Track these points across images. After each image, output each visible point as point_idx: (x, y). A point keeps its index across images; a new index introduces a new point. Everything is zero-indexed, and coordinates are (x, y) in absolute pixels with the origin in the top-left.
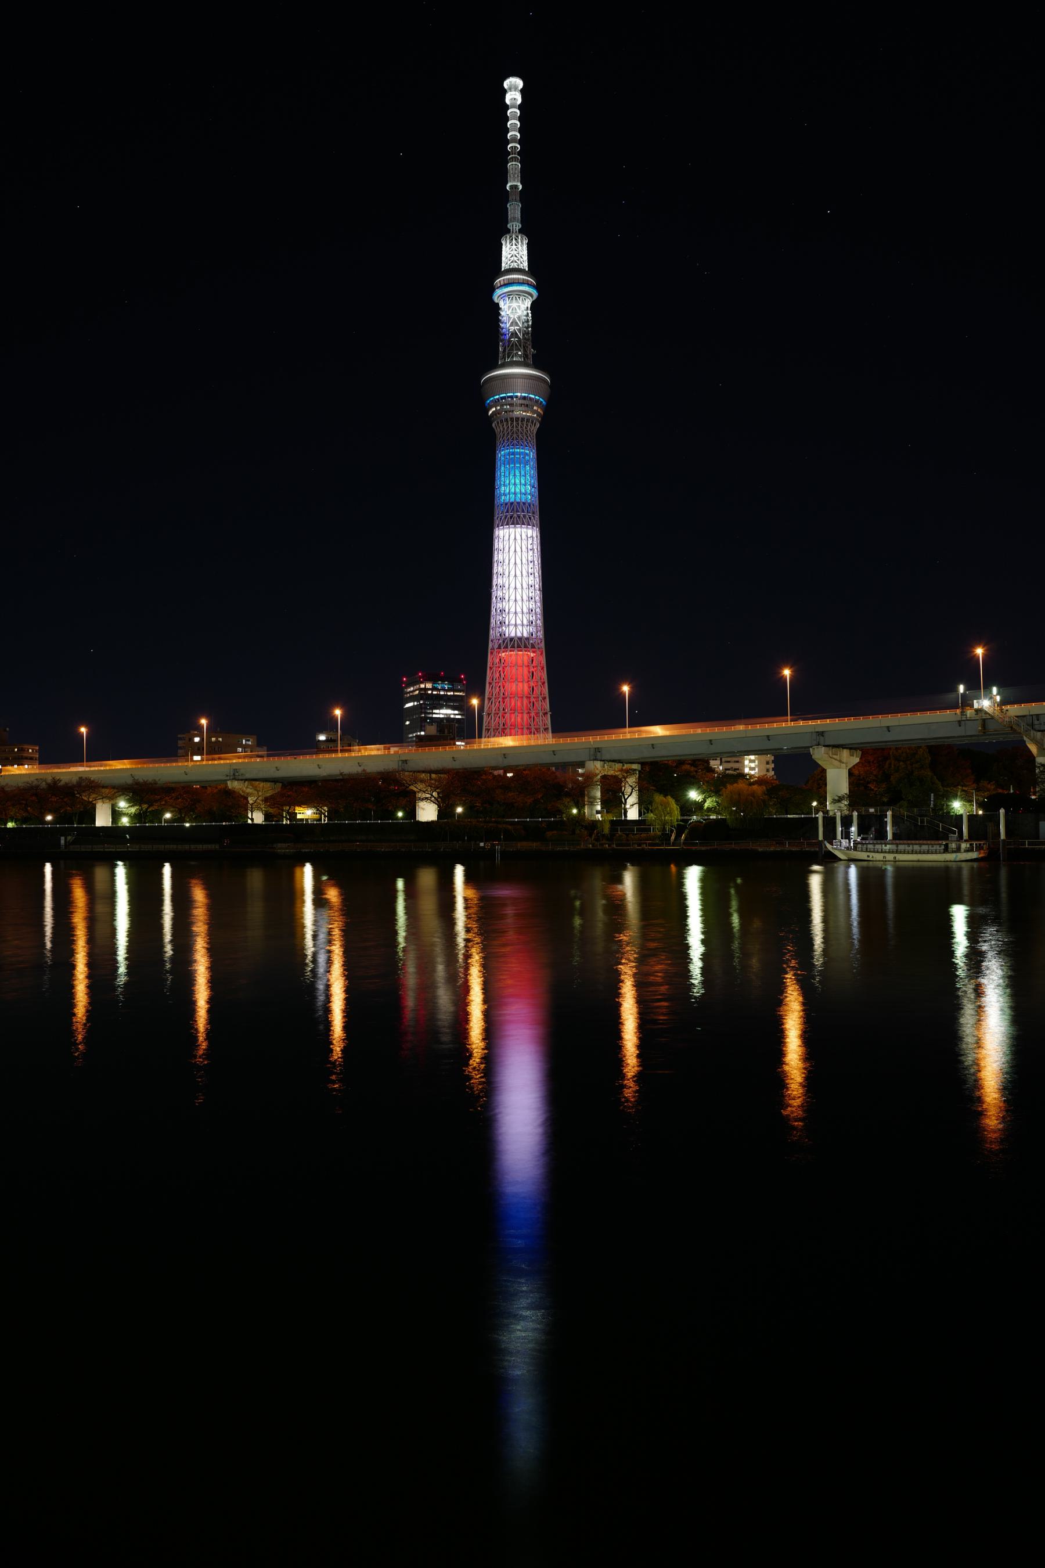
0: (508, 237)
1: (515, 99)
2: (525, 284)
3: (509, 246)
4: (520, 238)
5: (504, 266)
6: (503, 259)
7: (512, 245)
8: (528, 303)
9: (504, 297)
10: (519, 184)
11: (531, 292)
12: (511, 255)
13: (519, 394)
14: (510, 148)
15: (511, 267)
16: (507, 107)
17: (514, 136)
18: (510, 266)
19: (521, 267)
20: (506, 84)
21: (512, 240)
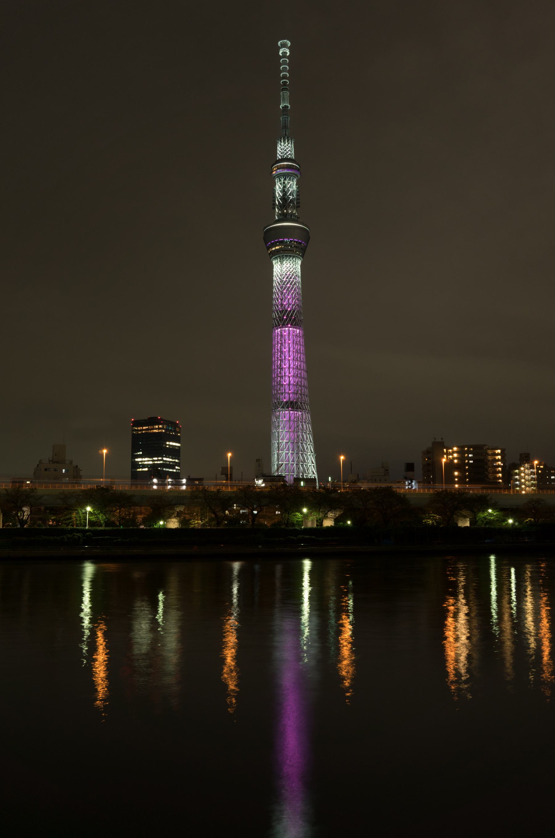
1: (285, 52)
2: (293, 169)
3: (282, 144)
4: (290, 138)
6: (278, 152)
7: (285, 143)
8: (295, 180)
9: (281, 176)
10: (288, 105)
11: (295, 173)
13: (286, 240)
14: (282, 82)
16: (281, 57)
17: (284, 75)
18: (284, 156)
20: (279, 43)
21: (285, 140)
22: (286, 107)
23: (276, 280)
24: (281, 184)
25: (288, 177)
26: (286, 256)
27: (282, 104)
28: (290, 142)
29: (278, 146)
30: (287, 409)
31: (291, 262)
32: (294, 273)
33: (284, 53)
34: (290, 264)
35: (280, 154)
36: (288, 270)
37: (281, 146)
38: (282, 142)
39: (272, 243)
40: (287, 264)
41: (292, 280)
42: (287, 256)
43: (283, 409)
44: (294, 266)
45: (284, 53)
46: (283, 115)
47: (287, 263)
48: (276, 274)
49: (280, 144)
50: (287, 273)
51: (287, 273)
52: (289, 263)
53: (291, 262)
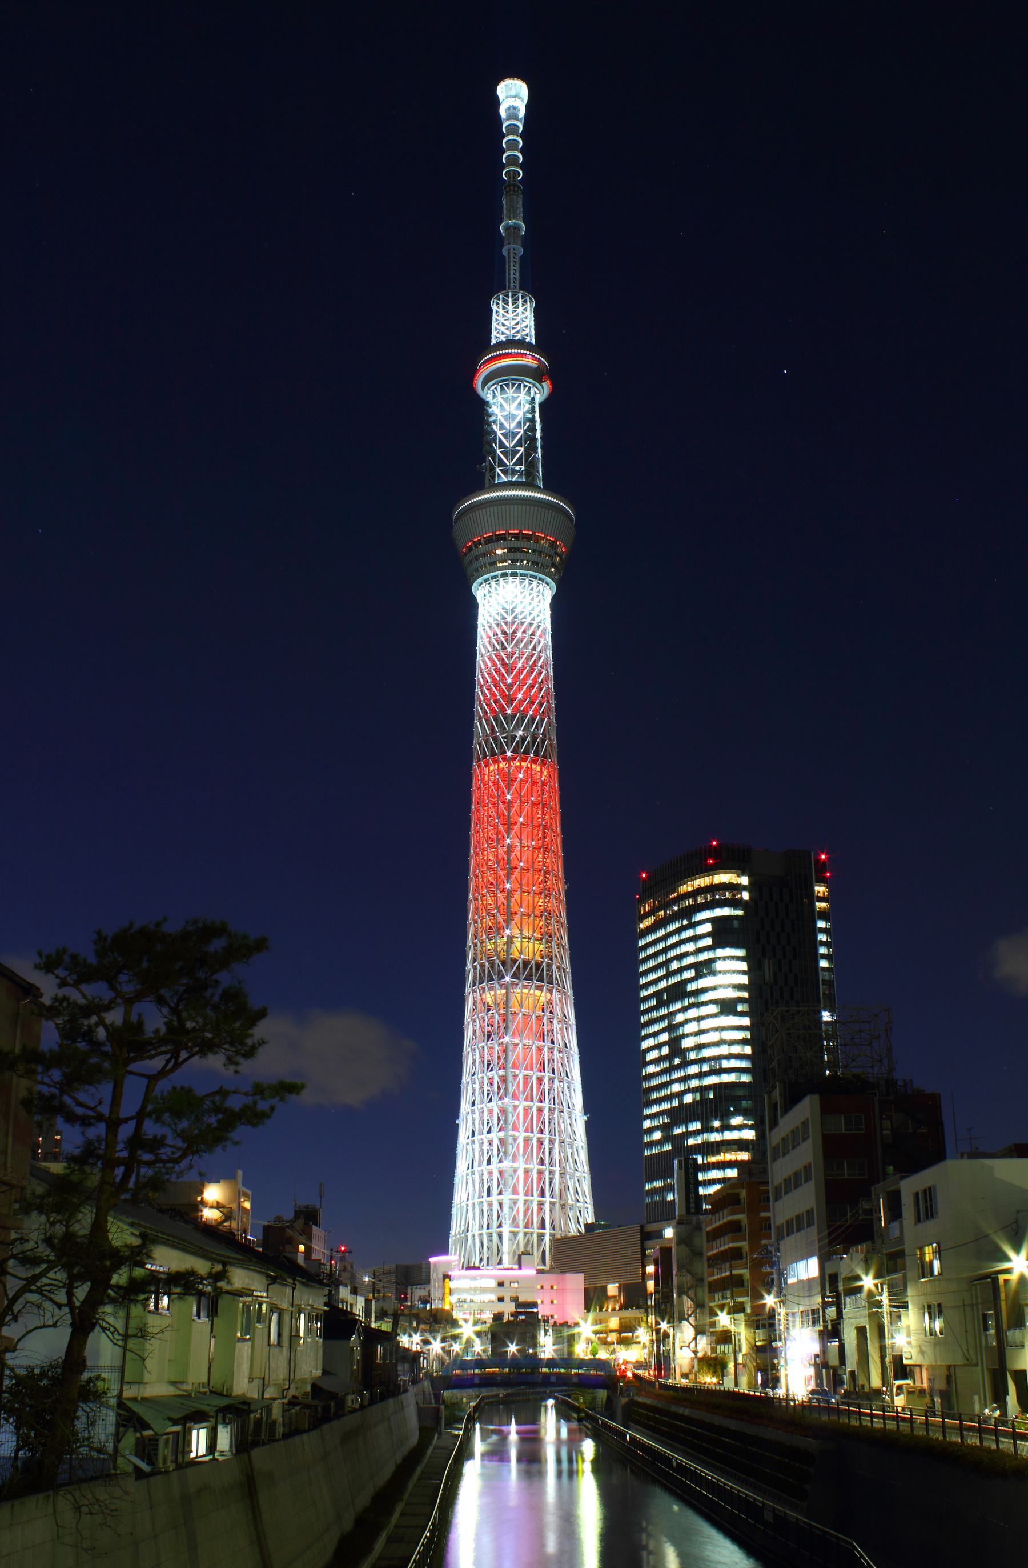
0: (510, 294)
1: (515, 108)
3: (510, 308)
4: (528, 300)
5: (497, 336)
7: (517, 307)
9: (507, 380)
12: (515, 322)
15: (516, 338)
19: (528, 339)
22: (517, 228)
23: (491, 634)
24: (506, 400)
25: (525, 386)
26: (522, 575)
27: (504, 216)
28: (529, 309)
29: (497, 312)
30: (525, 982)
31: (535, 594)
32: (540, 622)
33: (512, 113)
34: (533, 599)
35: (503, 329)
36: (526, 612)
37: (507, 312)
38: (510, 304)
39: (474, 542)
40: (524, 597)
41: (536, 638)
42: (525, 575)
43: (516, 981)
44: (541, 605)
45: (512, 113)
46: (509, 244)
47: (523, 595)
48: (491, 621)
49: (504, 308)
50: (523, 620)
51: (523, 620)
52: (530, 594)
53: (535, 594)
